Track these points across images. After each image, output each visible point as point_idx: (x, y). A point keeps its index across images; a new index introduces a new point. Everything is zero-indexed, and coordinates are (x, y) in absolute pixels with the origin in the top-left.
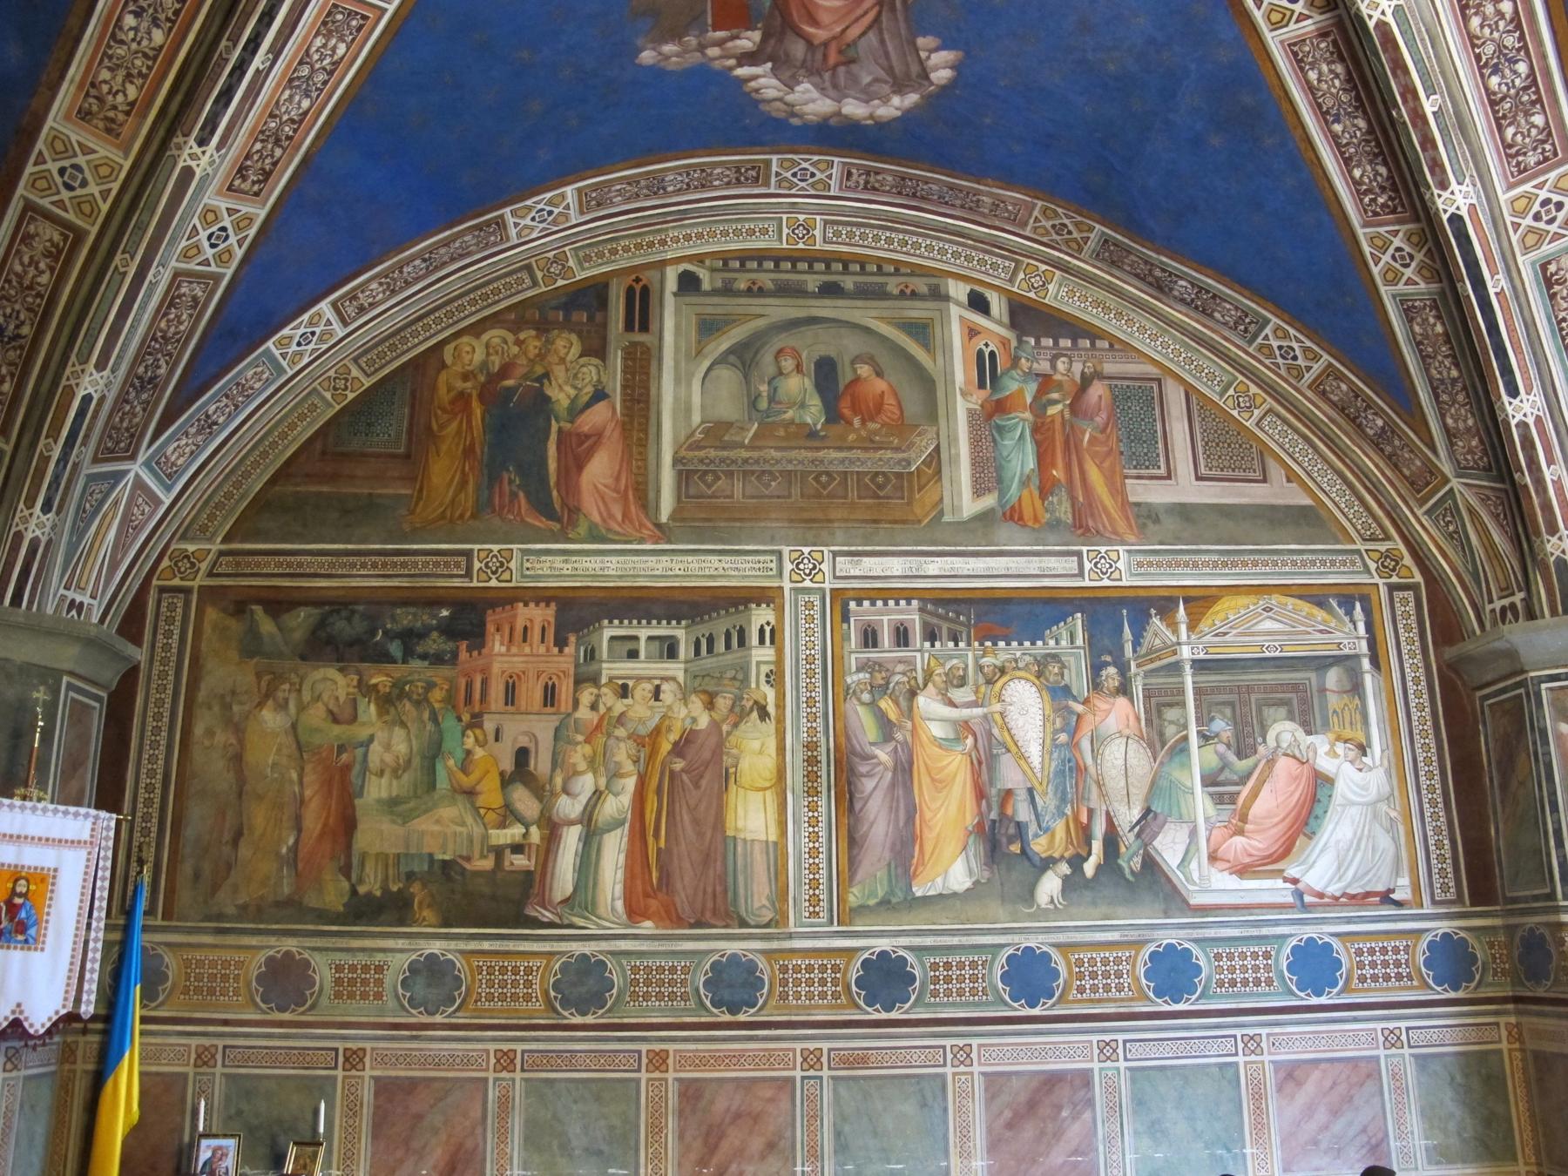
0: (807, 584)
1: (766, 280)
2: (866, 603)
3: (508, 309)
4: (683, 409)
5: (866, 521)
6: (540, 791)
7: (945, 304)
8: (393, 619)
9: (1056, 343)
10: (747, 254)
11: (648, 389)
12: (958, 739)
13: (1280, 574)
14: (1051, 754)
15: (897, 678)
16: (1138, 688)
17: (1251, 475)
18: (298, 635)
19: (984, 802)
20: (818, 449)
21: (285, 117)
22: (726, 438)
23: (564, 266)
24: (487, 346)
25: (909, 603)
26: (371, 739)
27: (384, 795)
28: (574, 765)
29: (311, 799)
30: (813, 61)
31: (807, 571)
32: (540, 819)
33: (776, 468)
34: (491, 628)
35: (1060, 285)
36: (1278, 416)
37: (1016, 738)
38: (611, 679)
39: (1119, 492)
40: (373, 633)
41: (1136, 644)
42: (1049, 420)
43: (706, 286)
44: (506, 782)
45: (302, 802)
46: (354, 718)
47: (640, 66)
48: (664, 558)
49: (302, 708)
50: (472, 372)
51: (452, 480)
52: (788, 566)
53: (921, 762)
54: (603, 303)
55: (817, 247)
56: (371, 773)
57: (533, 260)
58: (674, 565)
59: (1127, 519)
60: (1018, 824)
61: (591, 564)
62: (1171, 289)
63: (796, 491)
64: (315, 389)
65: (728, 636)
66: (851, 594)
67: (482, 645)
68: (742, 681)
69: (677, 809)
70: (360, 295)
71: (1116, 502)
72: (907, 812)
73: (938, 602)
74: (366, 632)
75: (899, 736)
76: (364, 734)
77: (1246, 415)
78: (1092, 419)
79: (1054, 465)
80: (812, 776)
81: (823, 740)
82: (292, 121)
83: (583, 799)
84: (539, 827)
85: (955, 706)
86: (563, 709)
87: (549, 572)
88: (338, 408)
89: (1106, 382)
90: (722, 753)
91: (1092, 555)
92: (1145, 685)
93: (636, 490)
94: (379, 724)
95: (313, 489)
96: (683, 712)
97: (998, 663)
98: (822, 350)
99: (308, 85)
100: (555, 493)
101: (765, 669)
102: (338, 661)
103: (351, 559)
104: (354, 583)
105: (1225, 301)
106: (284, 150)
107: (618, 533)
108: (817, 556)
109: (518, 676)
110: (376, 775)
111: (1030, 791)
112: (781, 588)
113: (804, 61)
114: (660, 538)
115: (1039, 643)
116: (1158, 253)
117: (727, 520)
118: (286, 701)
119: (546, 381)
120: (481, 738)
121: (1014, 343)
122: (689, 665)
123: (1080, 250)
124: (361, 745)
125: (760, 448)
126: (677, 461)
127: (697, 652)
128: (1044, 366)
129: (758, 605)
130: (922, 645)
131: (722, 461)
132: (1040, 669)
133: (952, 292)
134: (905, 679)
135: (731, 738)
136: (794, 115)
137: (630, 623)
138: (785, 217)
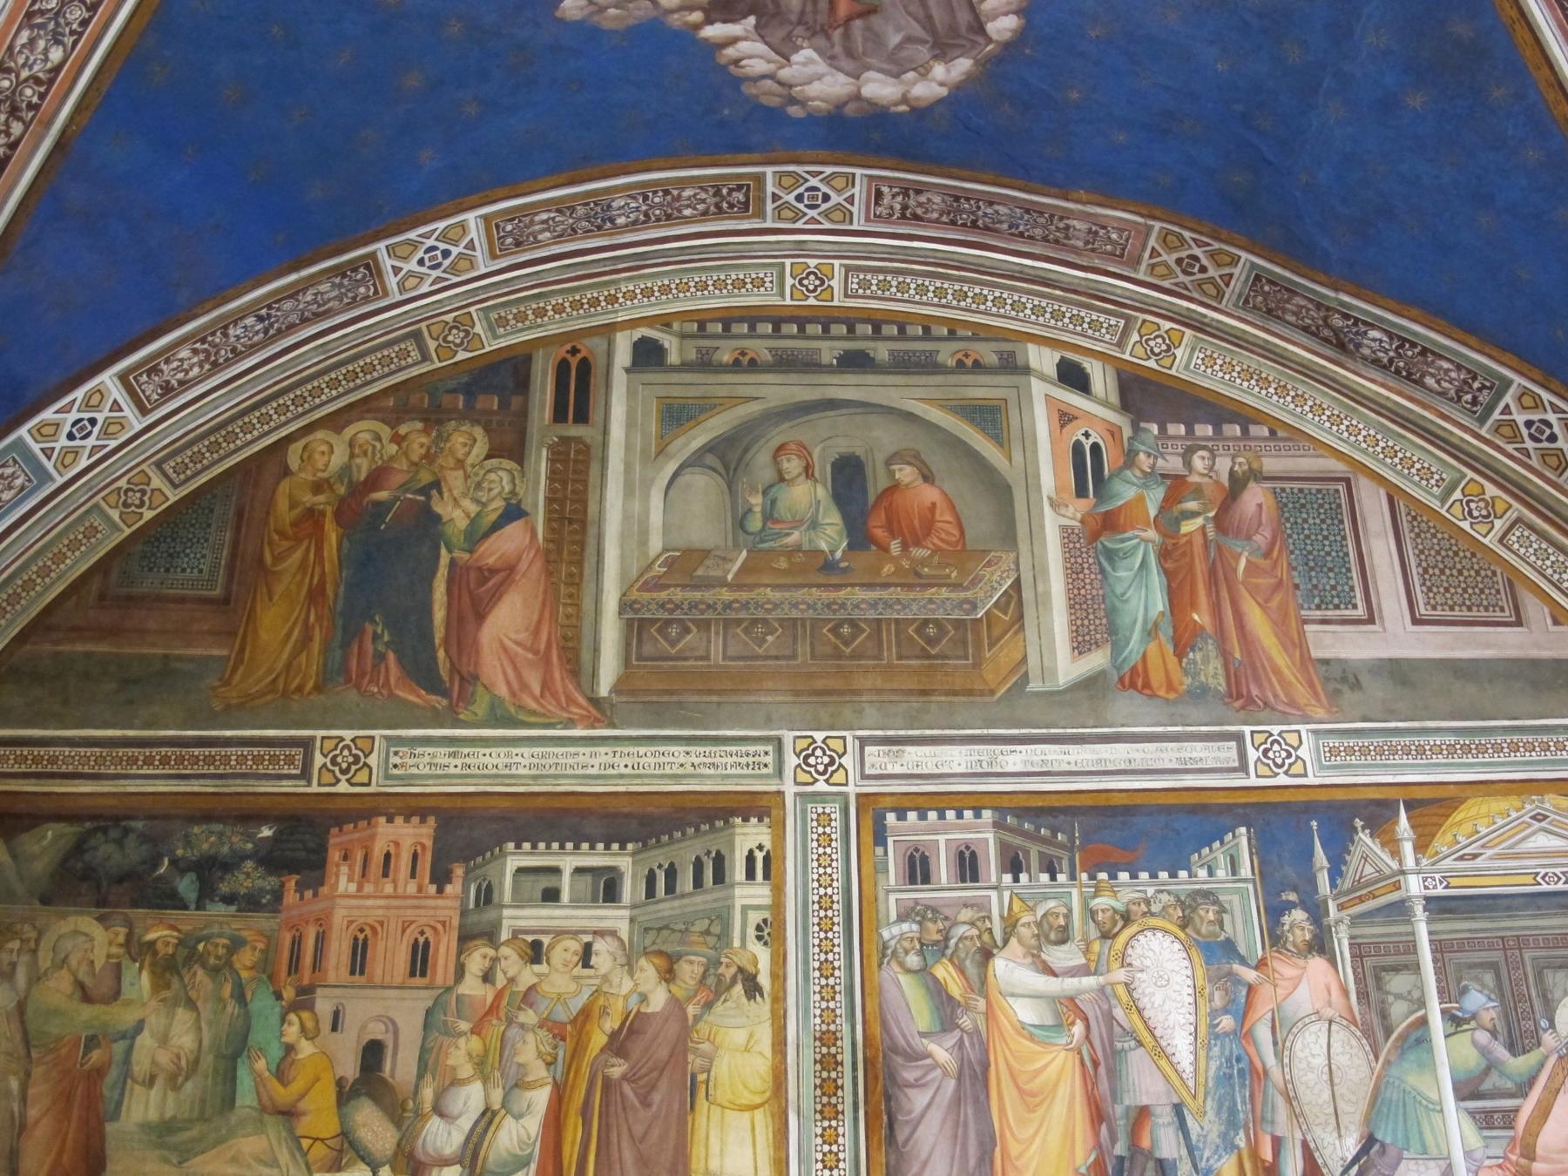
0: (821, 786)
1: (761, 349)
2: (912, 816)
3: (385, 392)
4: (637, 530)
5: (910, 692)
6: (399, 1111)
8: (188, 843)
9: (1190, 431)
10: (737, 313)
11: (584, 503)
12: (1060, 1026)
13: (1553, 762)
14: (1209, 1049)
15: (961, 930)
16: (1342, 942)
17: (1498, 615)
18: (41, 867)
19: (1104, 1128)
20: (838, 587)
21: (25, 74)
22: (700, 572)
23: (467, 333)
24: (351, 444)
25: (978, 815)
26: (139, 1027)
27: (153, 1115)
28: (454, 1069)
29: (37, 1121)
30: (815, 12)
31: (821, 768)
32: (396, 1155)
33: (774, 615)
34: (335, 855)
35: (1193, 349)
36: (1531, 528)
37: (1151, 1023)
38: (516, 933)
39: (1297, 645)
40: (155, 863)
41: (1335, 873)
42: (1183, 540)
43: (673, 358)
44: (346, 1095)
45: (23, 1127)
46: (117, 993)
47: (561, 21)
48: (602, 750)
49: (36, 978)
50: (327, 480)
51: (289, 635)
52: (791, 761)
53: (1002, 1066)
54: (522, 383)
55: (836, 303)
56: (135, 1081)
57: (423, 325)
58: (617, 760)
59: (1311, 685)
60: (1160, 1163)
61: (493, 759)
62: (1358, 346)
63: (803, 649)
64: (97, 506)
65: (698, 866)
66: (888, 802)
67: (321, 882)
68: (719, 937)
69: (614, 1139)
70: (164, 367)
71: (1291, 657)
72: (981, 1144)
73: (1023, 812)
74: (144, 862)
75: (965, 1021)
76: (128, 1018)
77: (1483, 529)
78: (1249, 538)
79: (1194, 605)
80: (827, 1088)
81: (846, 1029)
82: (38, 81)
83: (466, 1123)
85: (1054, 974)
86: (439, 980)
87: (427, 771)
88: (128, 531)
89: (1269, 485)
90: (685, 1051)
91: (1259, 738)
92: (1352, 937)
93: (563, 649)
94: (153, 1003)
95: (80, 648)
96: (627, 985)
97: (1119, 906)
98: (842, 446)
99: (57, 24)
100: (441, 654)
101: (755, 918)
102: (98, 905)
103: (130, 751)
104: (132, 787)
105: (1441, 357)
106: (27, 126)
107: (534, 713)
108: (837, 745)
109: (373, 929)
110: (143, 1083)
111: (1178, 1109)
112: (780, 793)
113: (803, 13)
114: (597, 720)
115: (1183, 874)
116: (1336, 290)
117: (699, 692)
118: (13, 965)
119: (434, 492)
120: (310, 1024)
121: (1127, 432)
122: (636, 912)
123: (1220, 296)
124: (123, 1036)
125: (751, 587)
126: (625, 606)
127: (651, 892)
128: (1174, 464)
129: (746, 820)
130: (1000, 879)
131: (694, 605)
132: (1186, 914)
133: (1034, 363)
134: (975, 932)
135: (700, 1025)
136: (793, 101)
137: (548, 847)
138: (788, 262)
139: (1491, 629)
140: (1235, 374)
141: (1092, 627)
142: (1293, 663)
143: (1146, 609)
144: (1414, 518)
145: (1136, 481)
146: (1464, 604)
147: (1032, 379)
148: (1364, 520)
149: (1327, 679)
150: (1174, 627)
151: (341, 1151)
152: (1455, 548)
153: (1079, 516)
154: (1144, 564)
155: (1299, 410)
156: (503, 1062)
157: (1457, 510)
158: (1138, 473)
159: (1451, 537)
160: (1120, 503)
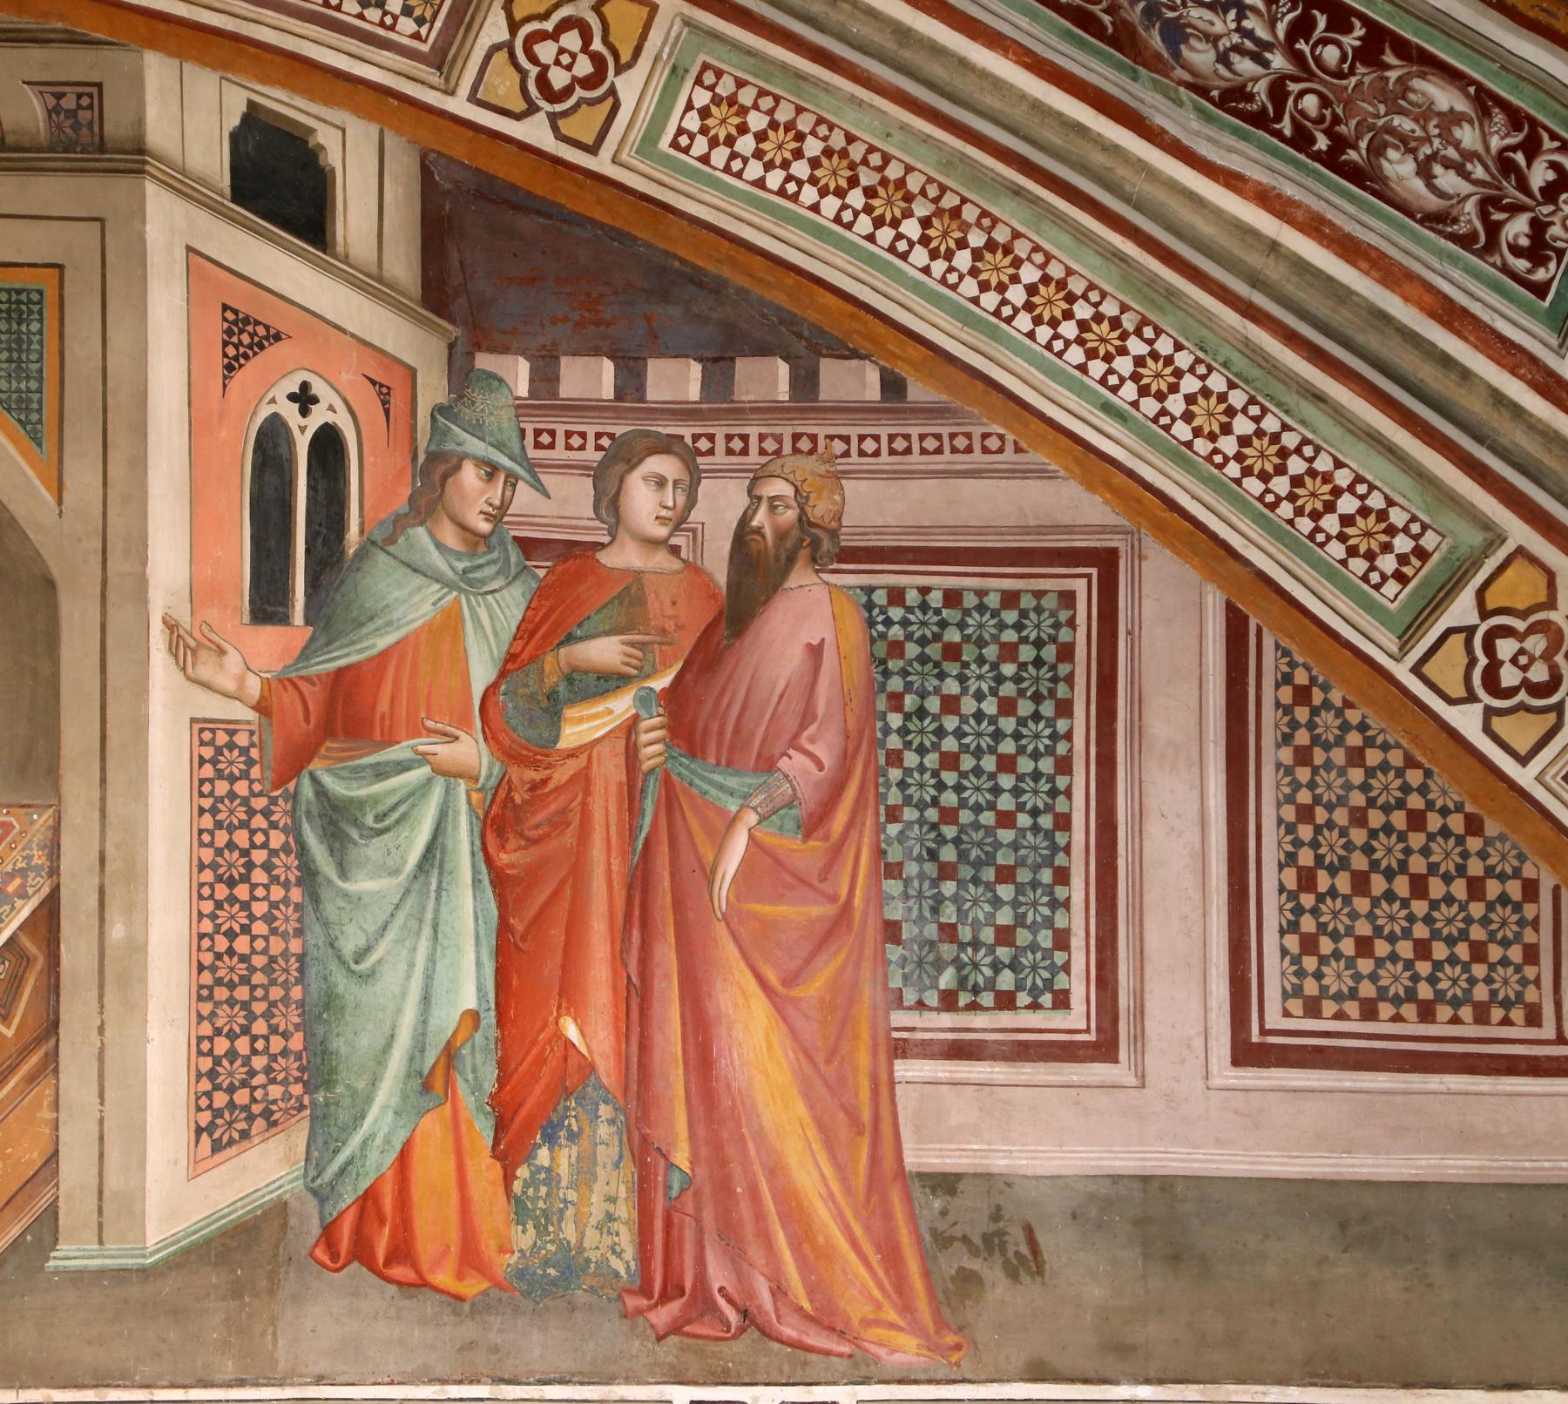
7: (120, 185)
9: (631, 383)
42: (562, 774)
59: (892, 1257)
78: (767, 764)
79: (570, 994)
121: (432, 389)
133: (159, 132)
139: (1483, 1083)
140: (801, 169)
141: (259, 1062)
142: (848, 1190)
143: (426, 1000)
144: (1302, 695)
145: (437, 560)
146: (1411, 995)
147: (151, 188)
148: (1137, 702)
149: (943, 1241)
150: (502, 1064)
152: (1415, 802)
153: (254, 687)
154: (434, 853)
155: (990, 300)
157: (1449, 667)
158: (450, 537)
159: (1411, 763)
160: (383, 643)
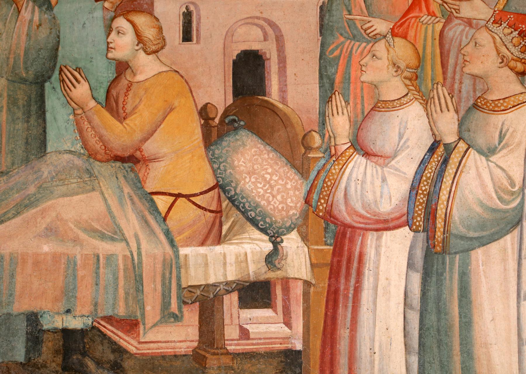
32: (305, 216)
84: (305, 238)
120: (149, 33)
151: (218, 212)
156: (449, 74)
